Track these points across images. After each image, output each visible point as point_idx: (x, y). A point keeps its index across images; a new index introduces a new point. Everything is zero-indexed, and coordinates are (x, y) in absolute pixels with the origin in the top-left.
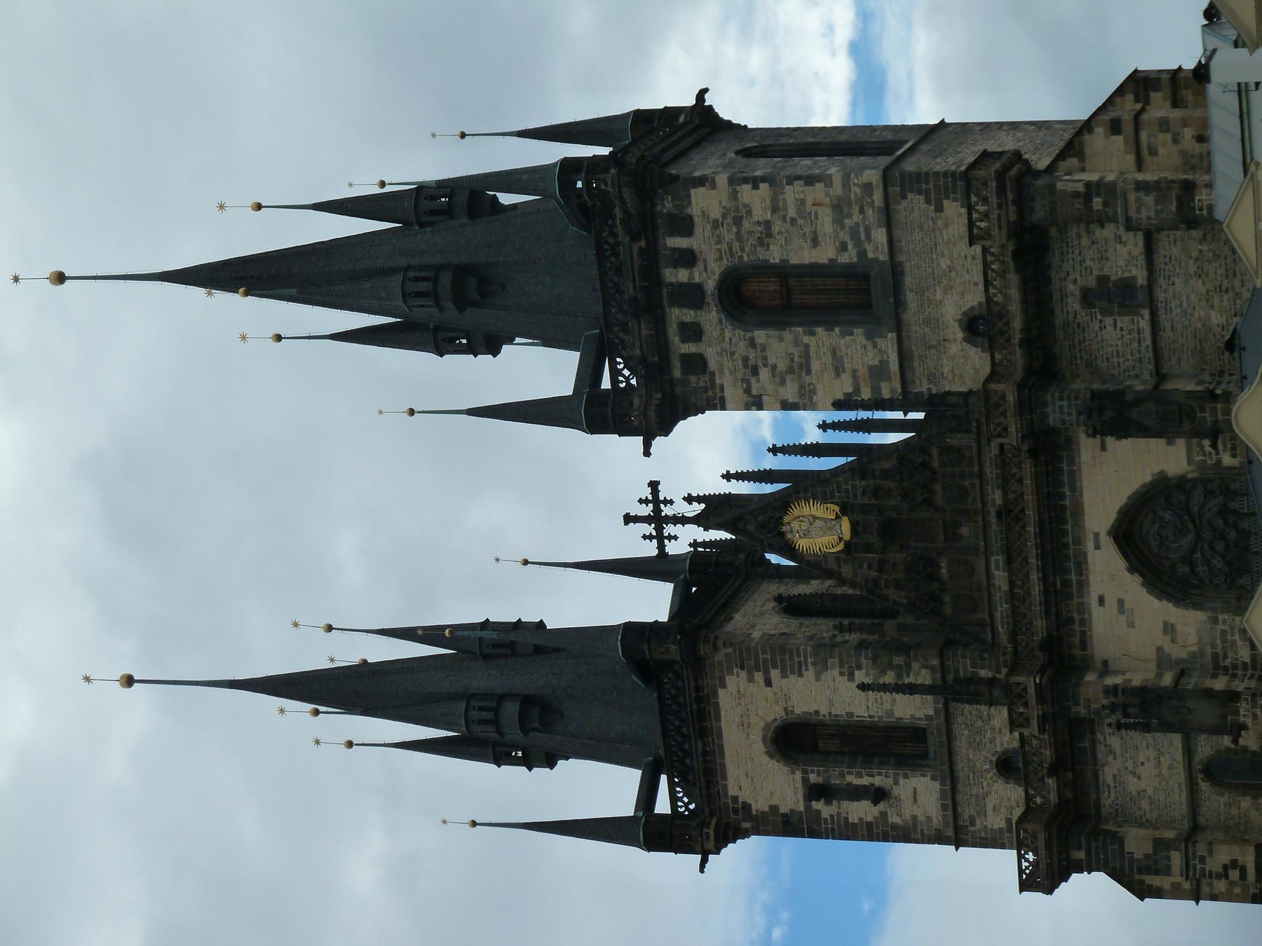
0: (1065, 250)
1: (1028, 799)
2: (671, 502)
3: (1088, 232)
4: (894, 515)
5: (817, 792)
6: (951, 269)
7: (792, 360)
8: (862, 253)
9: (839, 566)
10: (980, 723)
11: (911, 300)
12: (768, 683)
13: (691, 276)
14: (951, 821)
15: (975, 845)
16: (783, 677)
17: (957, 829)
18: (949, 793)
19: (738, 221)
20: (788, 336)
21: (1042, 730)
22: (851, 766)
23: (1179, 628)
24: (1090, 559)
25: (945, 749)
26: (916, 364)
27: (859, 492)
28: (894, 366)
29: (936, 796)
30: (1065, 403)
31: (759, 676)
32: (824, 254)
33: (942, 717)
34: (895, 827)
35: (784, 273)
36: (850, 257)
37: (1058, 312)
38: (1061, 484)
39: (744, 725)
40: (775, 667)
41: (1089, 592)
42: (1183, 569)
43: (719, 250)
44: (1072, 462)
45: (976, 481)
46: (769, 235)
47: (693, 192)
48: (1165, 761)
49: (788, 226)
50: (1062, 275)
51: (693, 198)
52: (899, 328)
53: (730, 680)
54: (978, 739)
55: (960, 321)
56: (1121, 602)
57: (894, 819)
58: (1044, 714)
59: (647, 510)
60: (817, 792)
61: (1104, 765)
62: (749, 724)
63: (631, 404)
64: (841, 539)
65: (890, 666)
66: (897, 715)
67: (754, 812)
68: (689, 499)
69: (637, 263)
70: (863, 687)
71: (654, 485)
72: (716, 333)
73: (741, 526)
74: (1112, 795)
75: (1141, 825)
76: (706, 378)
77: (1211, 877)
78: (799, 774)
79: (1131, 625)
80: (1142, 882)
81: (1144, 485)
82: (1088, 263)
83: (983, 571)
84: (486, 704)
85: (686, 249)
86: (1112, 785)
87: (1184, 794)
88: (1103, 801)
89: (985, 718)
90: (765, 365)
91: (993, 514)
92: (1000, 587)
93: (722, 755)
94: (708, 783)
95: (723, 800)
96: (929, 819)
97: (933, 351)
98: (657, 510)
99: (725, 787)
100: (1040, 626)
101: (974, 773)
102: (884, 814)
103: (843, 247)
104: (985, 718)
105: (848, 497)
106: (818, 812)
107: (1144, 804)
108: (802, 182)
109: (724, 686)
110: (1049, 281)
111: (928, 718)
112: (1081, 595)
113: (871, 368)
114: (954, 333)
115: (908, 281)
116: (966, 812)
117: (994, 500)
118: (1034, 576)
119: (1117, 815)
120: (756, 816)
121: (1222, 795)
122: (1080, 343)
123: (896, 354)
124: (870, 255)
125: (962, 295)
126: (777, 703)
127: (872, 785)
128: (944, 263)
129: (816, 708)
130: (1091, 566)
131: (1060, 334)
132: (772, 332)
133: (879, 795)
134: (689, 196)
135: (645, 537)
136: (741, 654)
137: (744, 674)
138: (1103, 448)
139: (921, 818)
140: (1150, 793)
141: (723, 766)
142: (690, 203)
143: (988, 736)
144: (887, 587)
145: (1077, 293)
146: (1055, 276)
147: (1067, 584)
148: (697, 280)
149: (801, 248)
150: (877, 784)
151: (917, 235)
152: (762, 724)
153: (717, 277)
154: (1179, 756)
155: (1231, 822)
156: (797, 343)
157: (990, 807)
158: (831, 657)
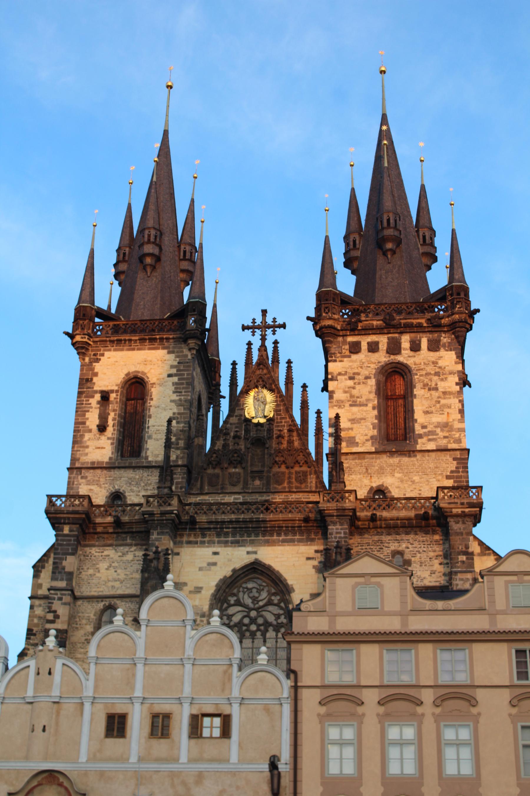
0: (426, 543)
1: (99, 506)
2: (274, 334)
3: (437, 556)
4: (267, 446)
5: (105, 397)
6: (413, 482)
7: (358, 397)
8: (420, 436)
9: (236, 416)
10: (143, 484)
11: (395, 460)
12: (170, 376)
13: (405, 349)
14: (85, 466)
15: (69, 478)
16: (173, 383)
17: (80, 469)
18: (102, 466)
19: (437, 374)
20: (373, 396)
21: (144, 513)
22: (120, 416)
23: (198, 596)
24: (241, 548)
25: (127, 465)
26: (357, 461)
27: (279, 428)
28: (355, 450)
29: (100, 459)
30: (342, 535)
31: (174, 371)
32: (419, 416)
33: (147, 465)
34: (82, 436)
35: (407, 397)
36: (418, 429)
37: (389, 537)
38: (286, 535)
39: (145, 362)
40: (179, 379)
41: (221, 547)
42: (232, 600)
43: (421, 364)
44: (300, 541)
45: (287, 490)
46: (429, 389)
47: (453, 352)
48: (117, 584)
49: (435, 399)
50: (411, 541)
51: (449, 352)
52: (376, 452)
53: (172, 356)
54: (133, 483)
55: (382, 485)
56: (215, 564)
57: (87, 436)
58: (154, 514)
59: (269, 320)
60: (105, 397)
61: (116, 550)
62: (146, 364)
63: (334, 314)
64: (253, 418)
65: (178, 439)
66: (149, 441)
67: (94, 364)
68: (276, 343)
69: (415, 321)
70: (169, 422)
71: (284, 326)
72: (373, 360)
73: (261, 366)
74: (97, 554)
75: (78, 569)
76: (347, 353)
77: (49, 603)
78: (116, 388)
79: (201, 569)
80: (43, 567)
81: (285, 580)
82: (418, 555)
83: (234, 491)
84: (158, 239)
85: (420, 347)
86: (103, 554)
87: (96, 594)
88: (94, 549)
89: (146, 488)
90: (355, 384)
91: (267, 498)
92: (224, 499)
93: (129, 350)
94: (112, 342)
95: (102, 349)
96: (87, 454)
97: (364, 470)
98: (269, 327)
99: (110, 350)
100: (202, 518)
101: (113, 480)
102: (90, 431)
103: (424, 427)
104: (146, 488)
105: (277, 423)
106: (93, 397)
107: (91, 571)
108: (461, 407)
109: (169, 353)
110: (407, 533)
111: (147, 458)
112: (219, 542)
113: (354, 437)
114: (375, 482)
115: (405, 460)
116: (90, 474)
117: (276, 499)
118: (233, 517)
119: (84, 556)
120: (92, 365)
121: (94, 615)
122: (370, 549)
123: (362, 451)
124: (420, 441)
125: (398, 487)
126: (158, 379)
127: (108, 426)
128: (416, 478)
129: (154, 399)
130: (237, 549)
131: (376, 538)
132: (374, 388)
133: (102, 428)
134: (451, 350)
135: (254, 320)
136: (187, 363)
137: (176, 363)
138: (308, 559)
139: (87, 450)
140: (98, 575)
141: (122, 350)
142: (447, 351)
143: (135, 488)
144: (225, 440)
145: (400, 549)
146: (411, 537)
147: (226, 535)
148: (403, 352)
149: (423, 405)
150: (108, 428)
151: (432, 465)
152: (146, 371)
153: (405, 362)
154: (120, 592)
155: (78, 619)
156: (368, 400)
157: (92, 487)
158: (184, 409)
